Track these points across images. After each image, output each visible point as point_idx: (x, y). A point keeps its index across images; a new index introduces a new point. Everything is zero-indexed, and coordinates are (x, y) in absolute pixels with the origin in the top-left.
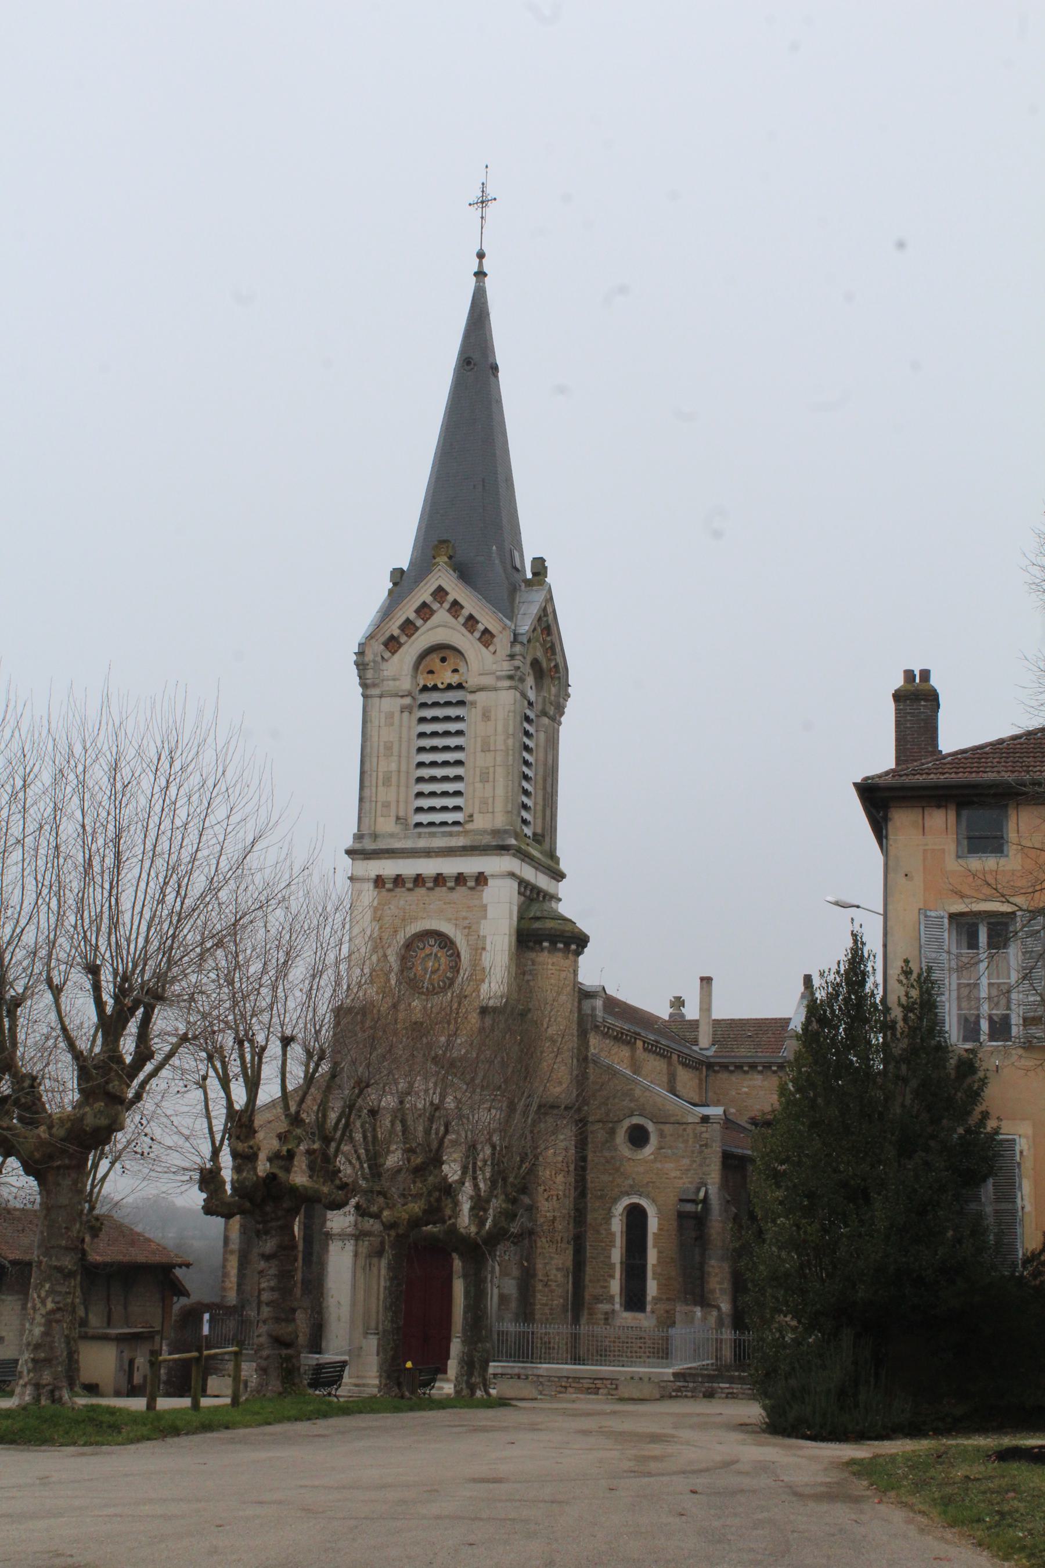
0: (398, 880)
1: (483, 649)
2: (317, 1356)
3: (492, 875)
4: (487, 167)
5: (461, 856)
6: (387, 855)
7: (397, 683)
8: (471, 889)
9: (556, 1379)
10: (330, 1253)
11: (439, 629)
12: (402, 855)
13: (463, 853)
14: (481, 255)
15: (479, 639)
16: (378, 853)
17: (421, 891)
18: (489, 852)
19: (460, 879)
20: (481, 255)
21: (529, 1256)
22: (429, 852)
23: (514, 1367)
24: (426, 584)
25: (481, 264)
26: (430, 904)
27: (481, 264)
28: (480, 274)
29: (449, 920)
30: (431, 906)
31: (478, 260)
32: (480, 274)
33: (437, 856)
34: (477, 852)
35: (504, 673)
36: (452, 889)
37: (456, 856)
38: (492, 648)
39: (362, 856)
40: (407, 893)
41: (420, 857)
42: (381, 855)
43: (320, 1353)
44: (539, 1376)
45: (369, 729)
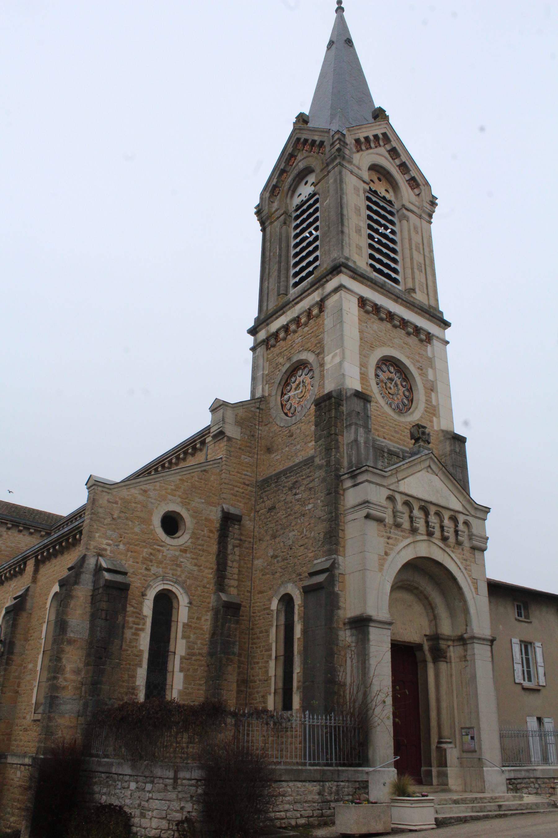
0: (377, 309)
1: (409, 189)
2: (366, 769)
3: (437, 337)
5: (416, 313)
6: (369, 283)
7: (360, 172)
8: (421, 341)
9: (547, 781)
10: (371, 643)
11: (383, 158)
12: (379, 289)
13: (419, 311)
15: (407, 181)
16: (364, 278)
17: (389, 326)
18: (434, 319)
19: (417, 330)
21: (451, 665)
22: (399, 298)
23: (521, 770)
24: (379, 125)
26: (394, 338)
29: (408, 358)
30: (395, 340)
33: (401, 304)
34: (427, 316)
35: (427, 210)
36: (409, 334)
37: (413, 311)
38: (417, 191)
39: (351, 274)
40: (378, 321)
41: (390, 298)
42: (365, 281)
43: (368, 766)
44: (537, 778)
45: (345, 188)
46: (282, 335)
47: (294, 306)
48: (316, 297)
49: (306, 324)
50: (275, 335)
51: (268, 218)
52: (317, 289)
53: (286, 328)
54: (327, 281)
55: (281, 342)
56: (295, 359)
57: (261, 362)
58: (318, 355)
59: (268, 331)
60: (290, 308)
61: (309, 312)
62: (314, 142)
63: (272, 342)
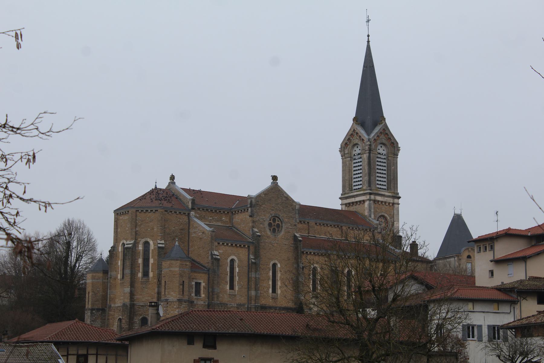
4: (367, 10)
14: (368, 36)
20: (368, 36)
25: (368, 39)
27: (368, 39)
28: (368, 42)
31: (367, 37)
32: (368, 42)
46: (380, 203)
47: (384, 197)
48: (391, 200)
49: (387, 206)
50: (378, 201)
51: (372, 151)
52: (392, 198)
53: (382, 202)
54: (395, 199)
55: (378, 204)
56: (383, 214)
57: (373, 206)
58: (390, 218)
59: (375, 198)
60: (383, 197)
61: (389, 203)
62: (390, 138)
63: (376, 202)
